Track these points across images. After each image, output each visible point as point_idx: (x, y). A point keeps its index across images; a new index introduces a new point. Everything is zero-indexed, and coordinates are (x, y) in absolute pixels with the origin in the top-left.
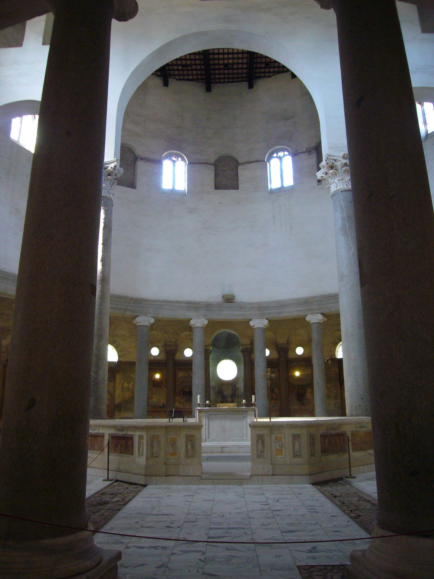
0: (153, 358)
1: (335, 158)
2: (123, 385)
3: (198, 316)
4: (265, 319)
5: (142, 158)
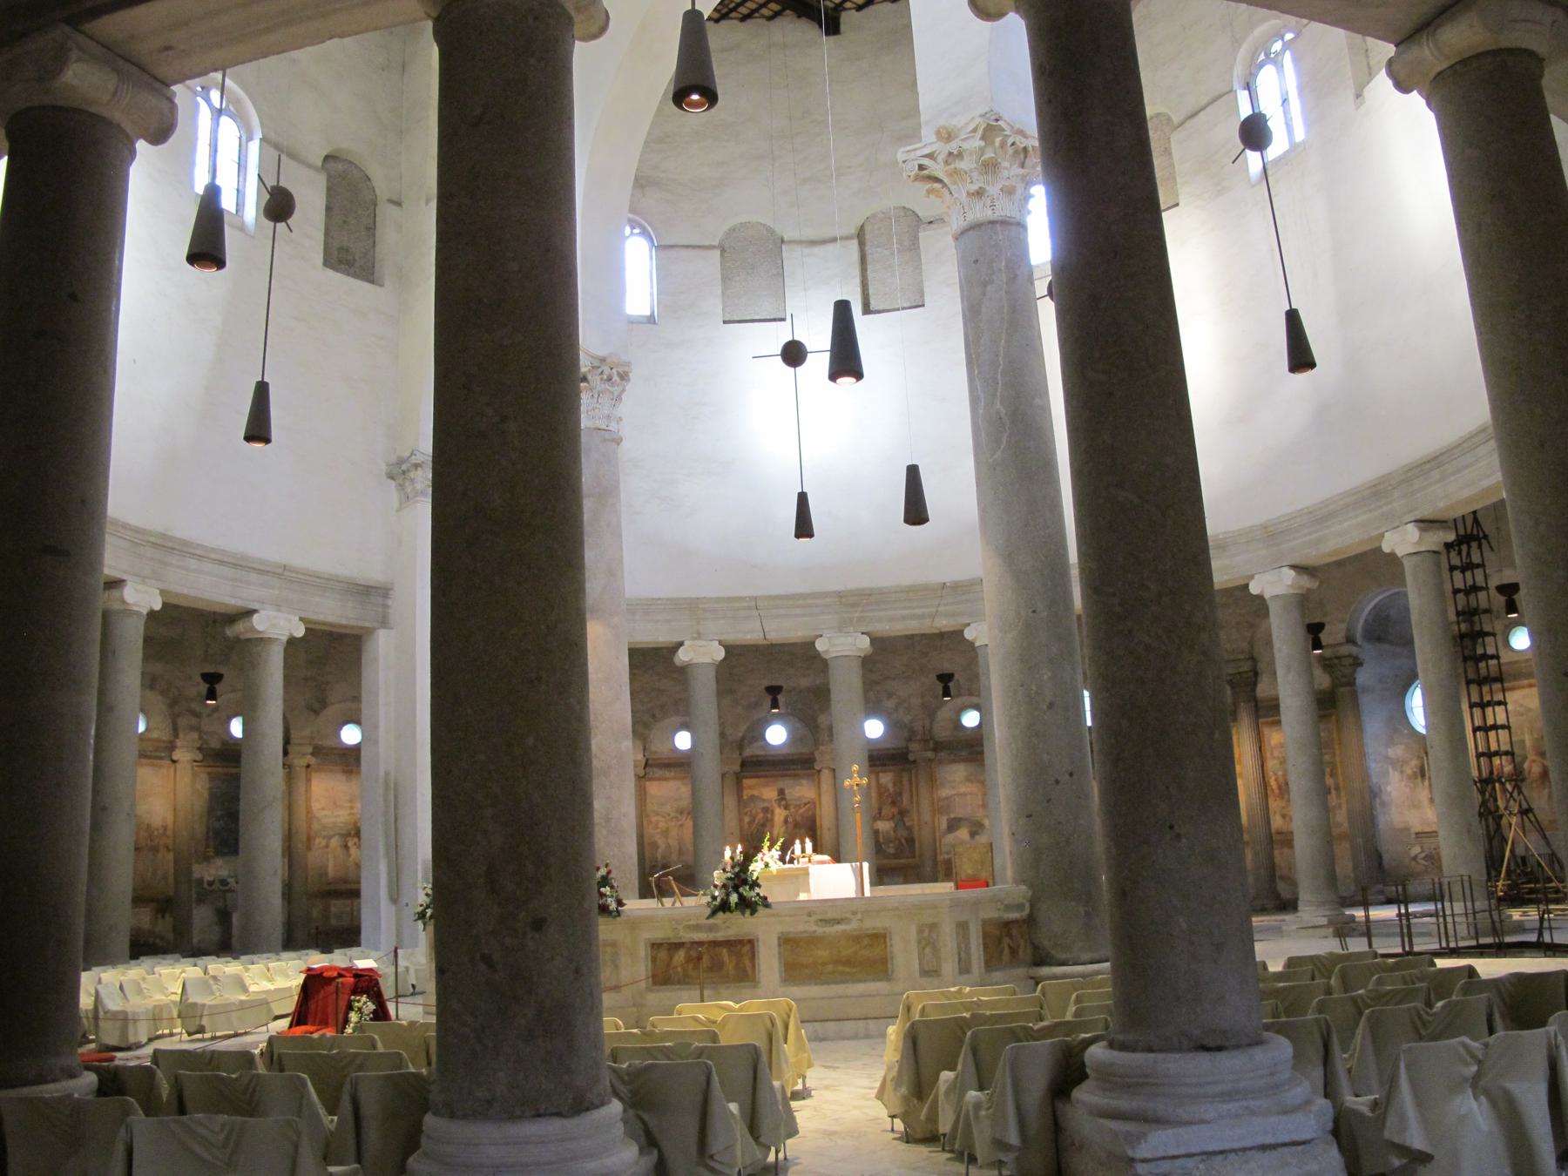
1: (926, 151)
4: (1286, 569)
5: (931, 225)
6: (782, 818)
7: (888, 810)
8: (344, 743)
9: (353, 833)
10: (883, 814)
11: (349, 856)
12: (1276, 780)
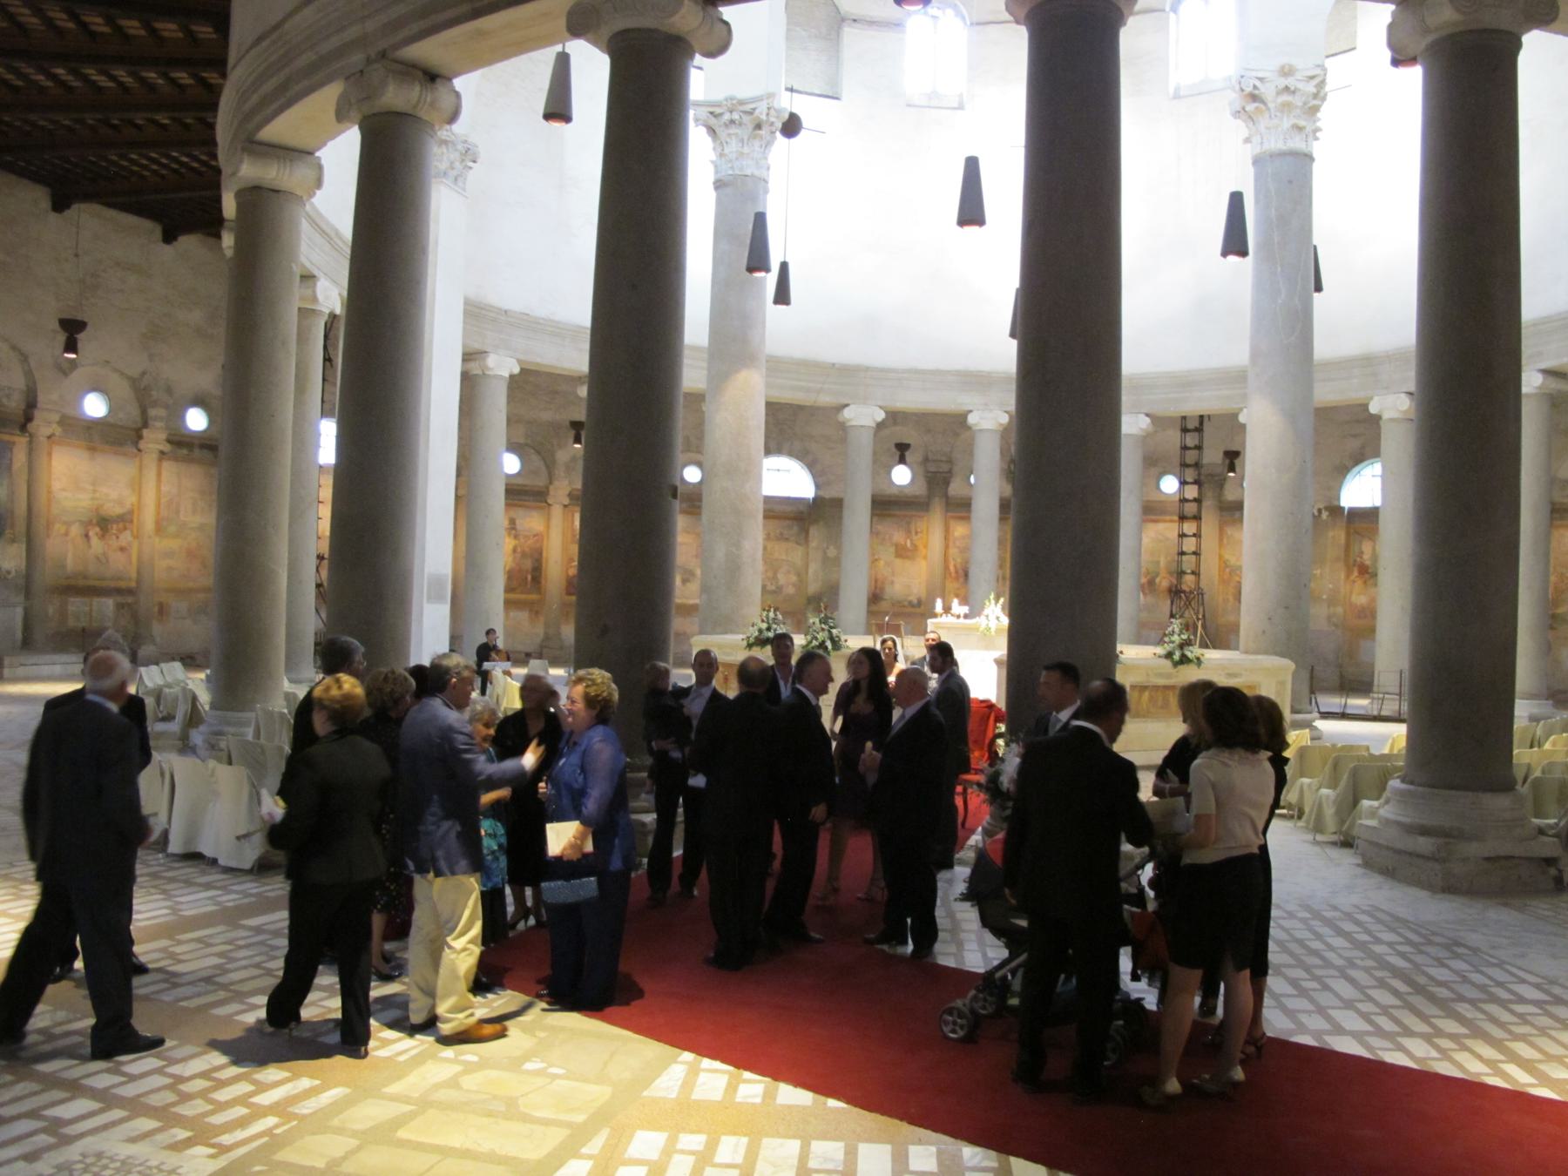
0: (894, 491)
1: (1260, 75)
2: (825, 553)
3: (986, 405)
4: (1142, 416)
5: (855, 18)
6: (511, 547)
8: (84, 414)
9: (94, 521)
11: (90, 547)
12: (955, 566)
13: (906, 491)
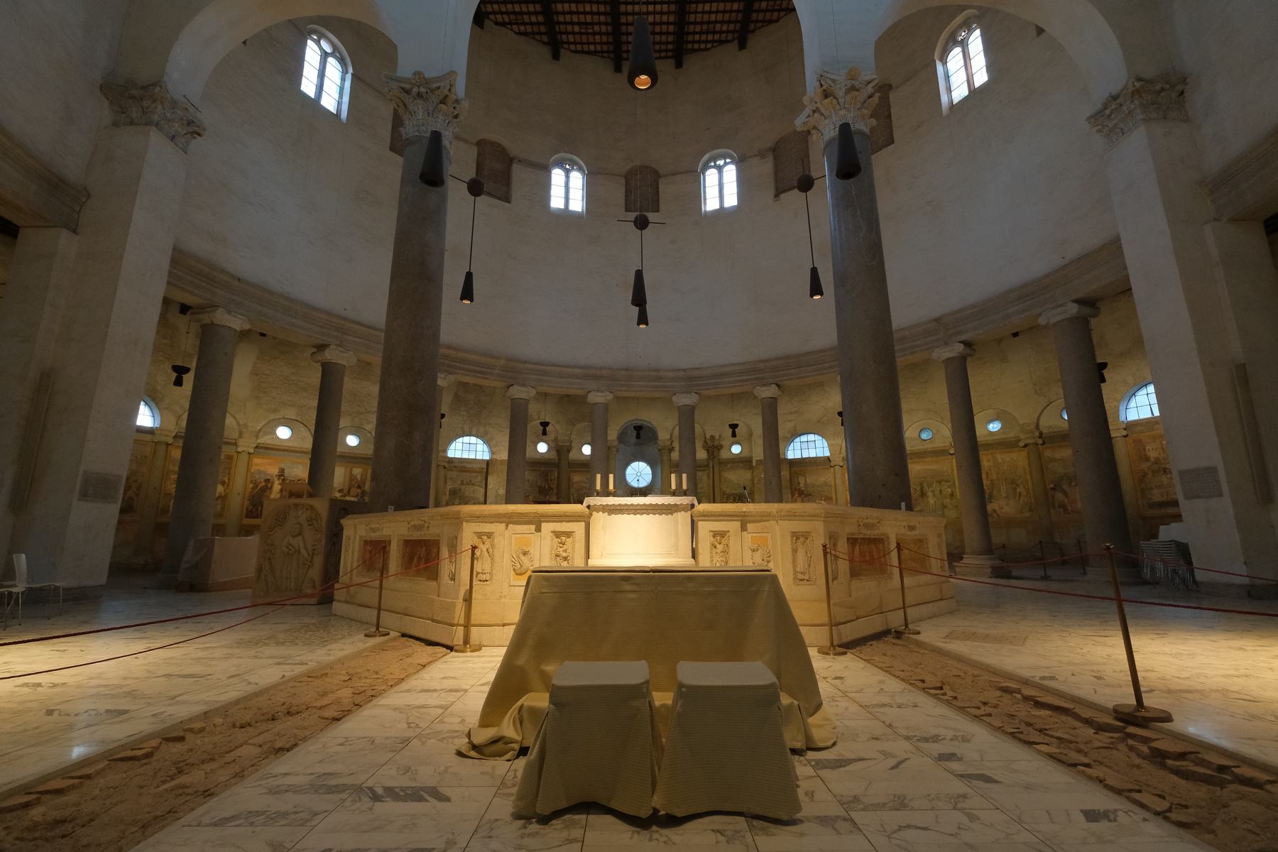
0: (539, 457)
7: (354, 491)
10: (351, 492)
13: (546, 456)
